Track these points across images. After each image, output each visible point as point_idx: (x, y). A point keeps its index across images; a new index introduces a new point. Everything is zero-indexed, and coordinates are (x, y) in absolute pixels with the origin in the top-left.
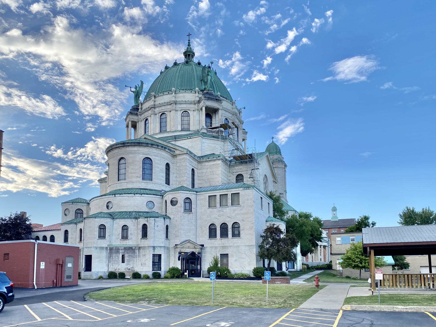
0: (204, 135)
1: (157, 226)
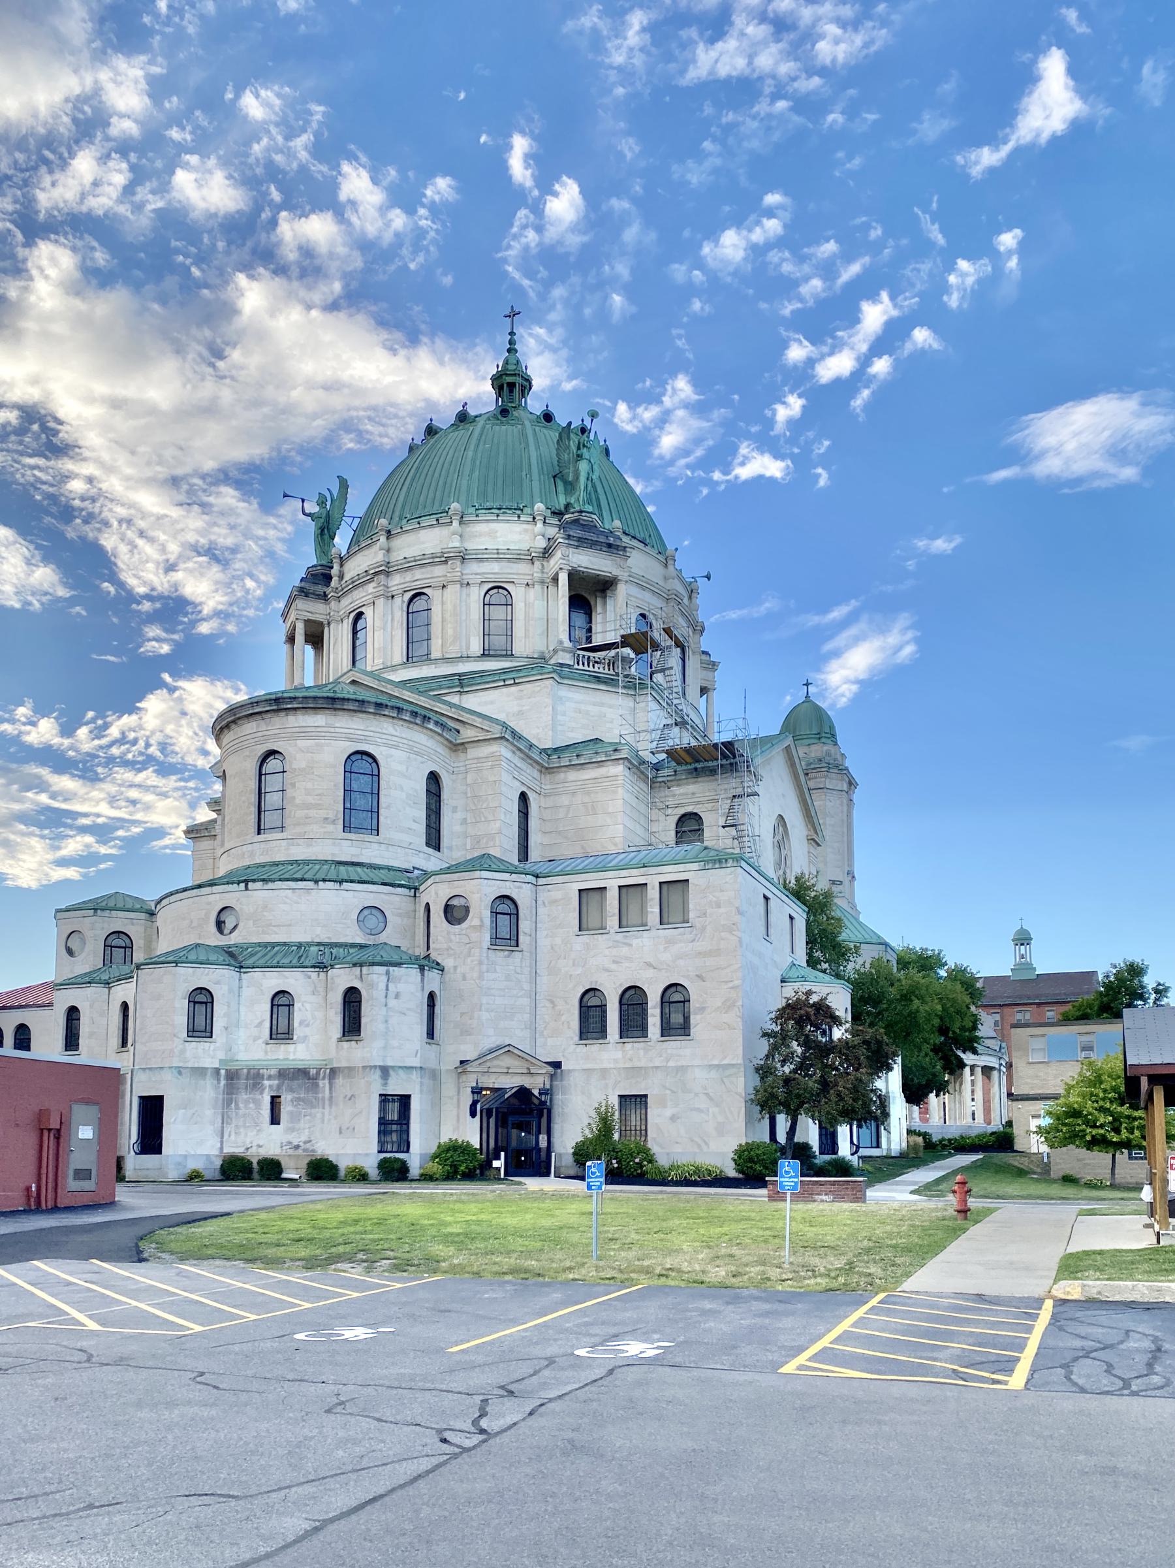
0: (562, 672)
1: (397, 996)
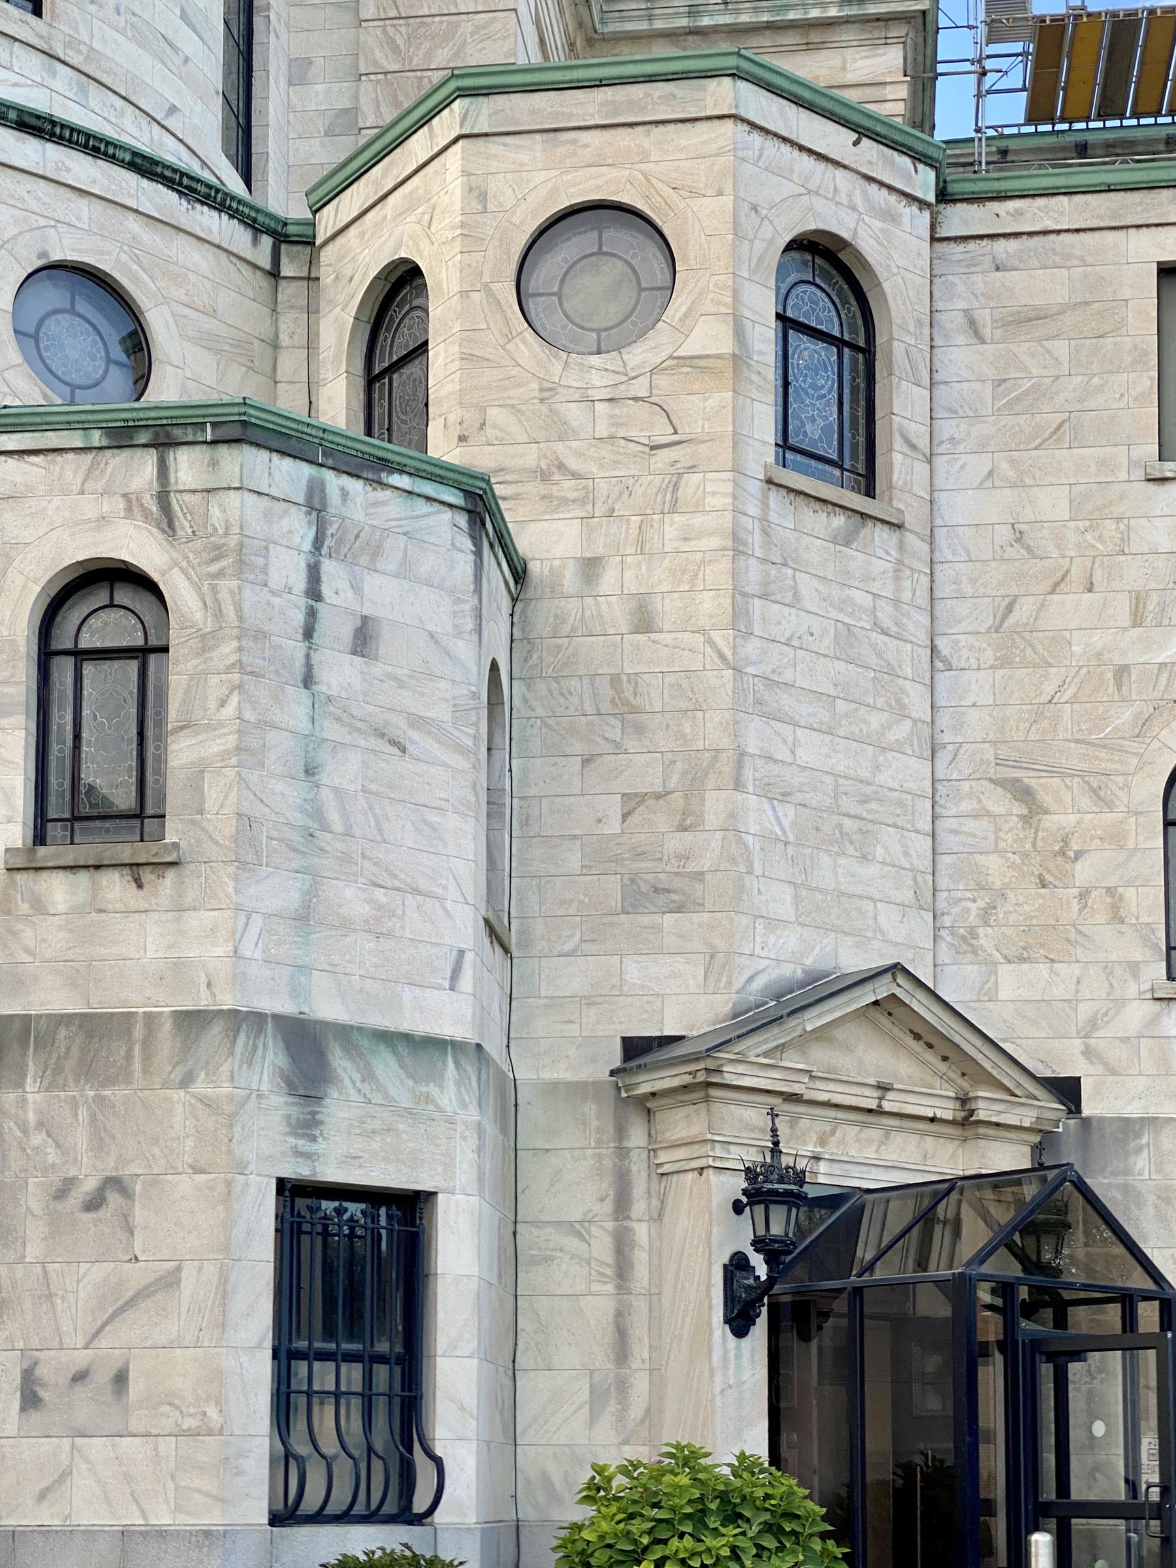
1: (363, 639)
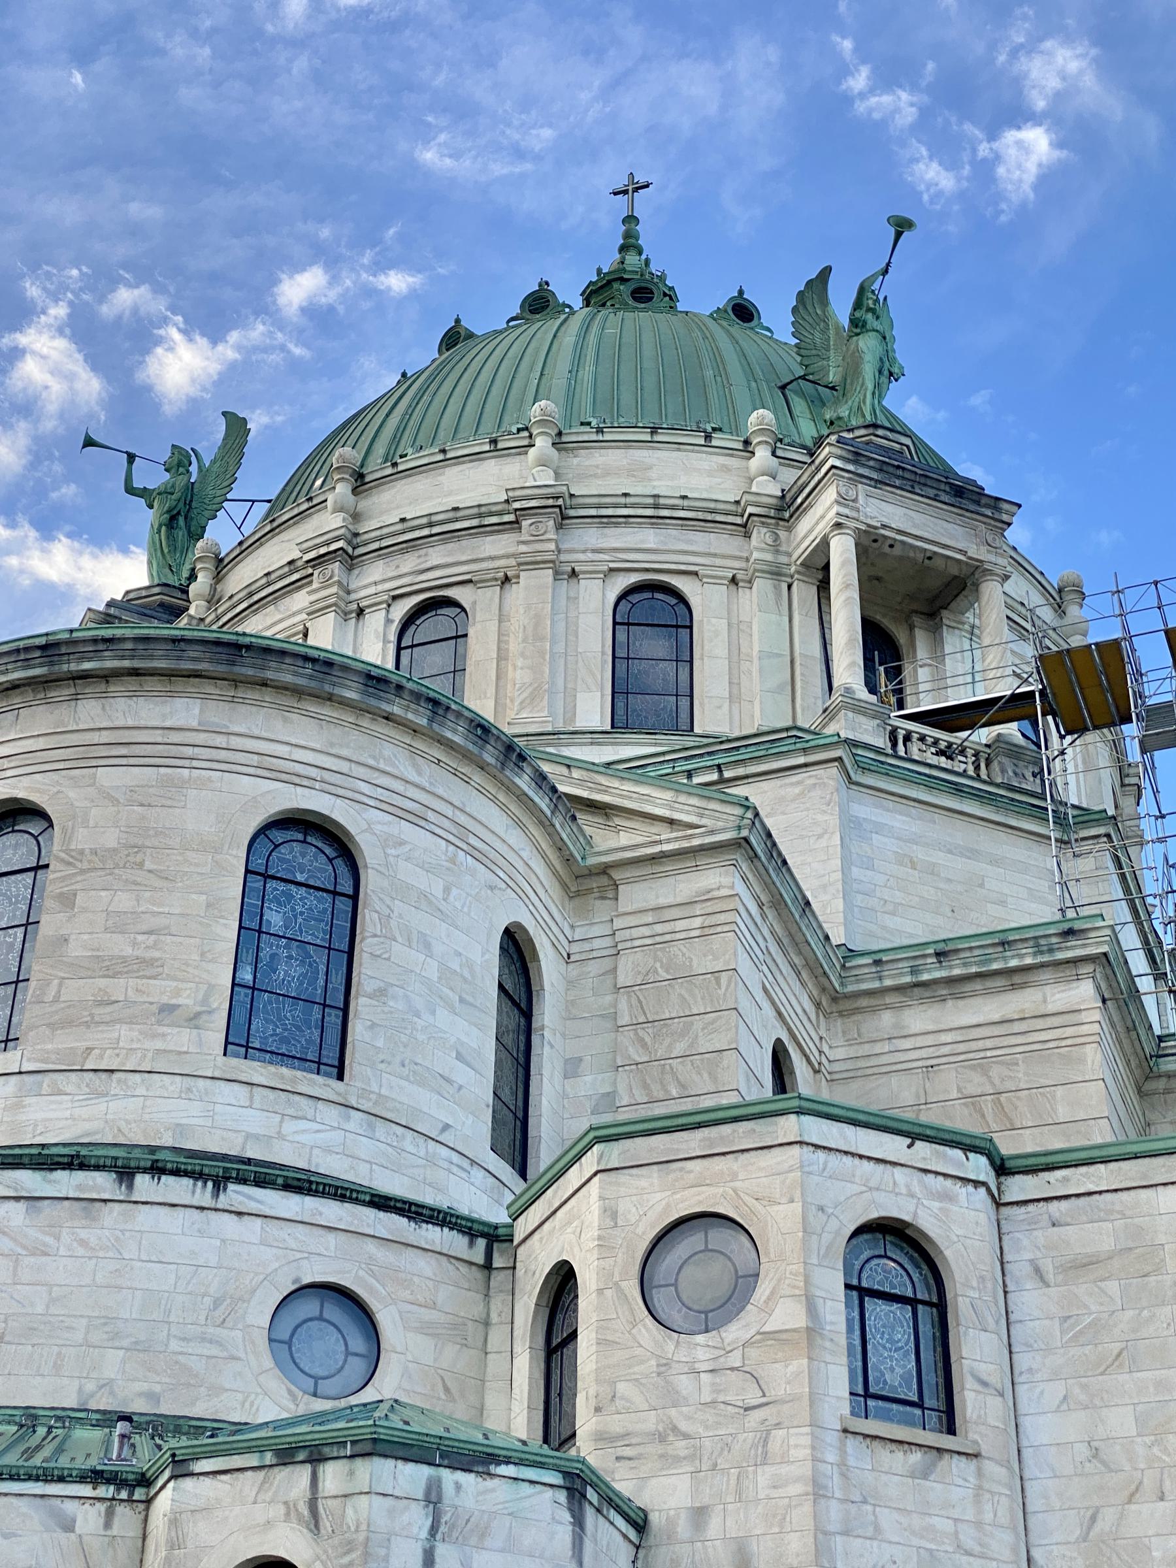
0: (858, 765)
